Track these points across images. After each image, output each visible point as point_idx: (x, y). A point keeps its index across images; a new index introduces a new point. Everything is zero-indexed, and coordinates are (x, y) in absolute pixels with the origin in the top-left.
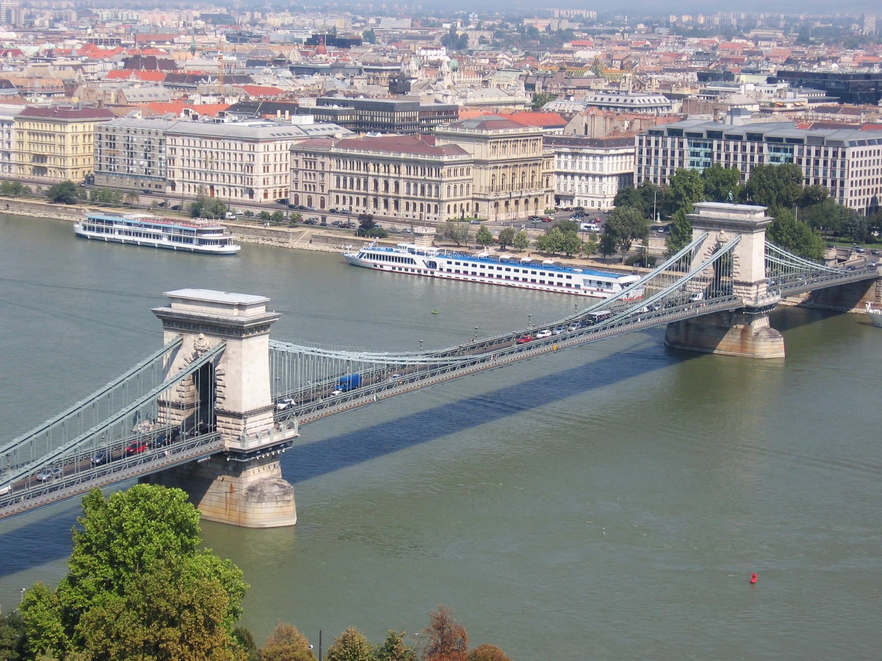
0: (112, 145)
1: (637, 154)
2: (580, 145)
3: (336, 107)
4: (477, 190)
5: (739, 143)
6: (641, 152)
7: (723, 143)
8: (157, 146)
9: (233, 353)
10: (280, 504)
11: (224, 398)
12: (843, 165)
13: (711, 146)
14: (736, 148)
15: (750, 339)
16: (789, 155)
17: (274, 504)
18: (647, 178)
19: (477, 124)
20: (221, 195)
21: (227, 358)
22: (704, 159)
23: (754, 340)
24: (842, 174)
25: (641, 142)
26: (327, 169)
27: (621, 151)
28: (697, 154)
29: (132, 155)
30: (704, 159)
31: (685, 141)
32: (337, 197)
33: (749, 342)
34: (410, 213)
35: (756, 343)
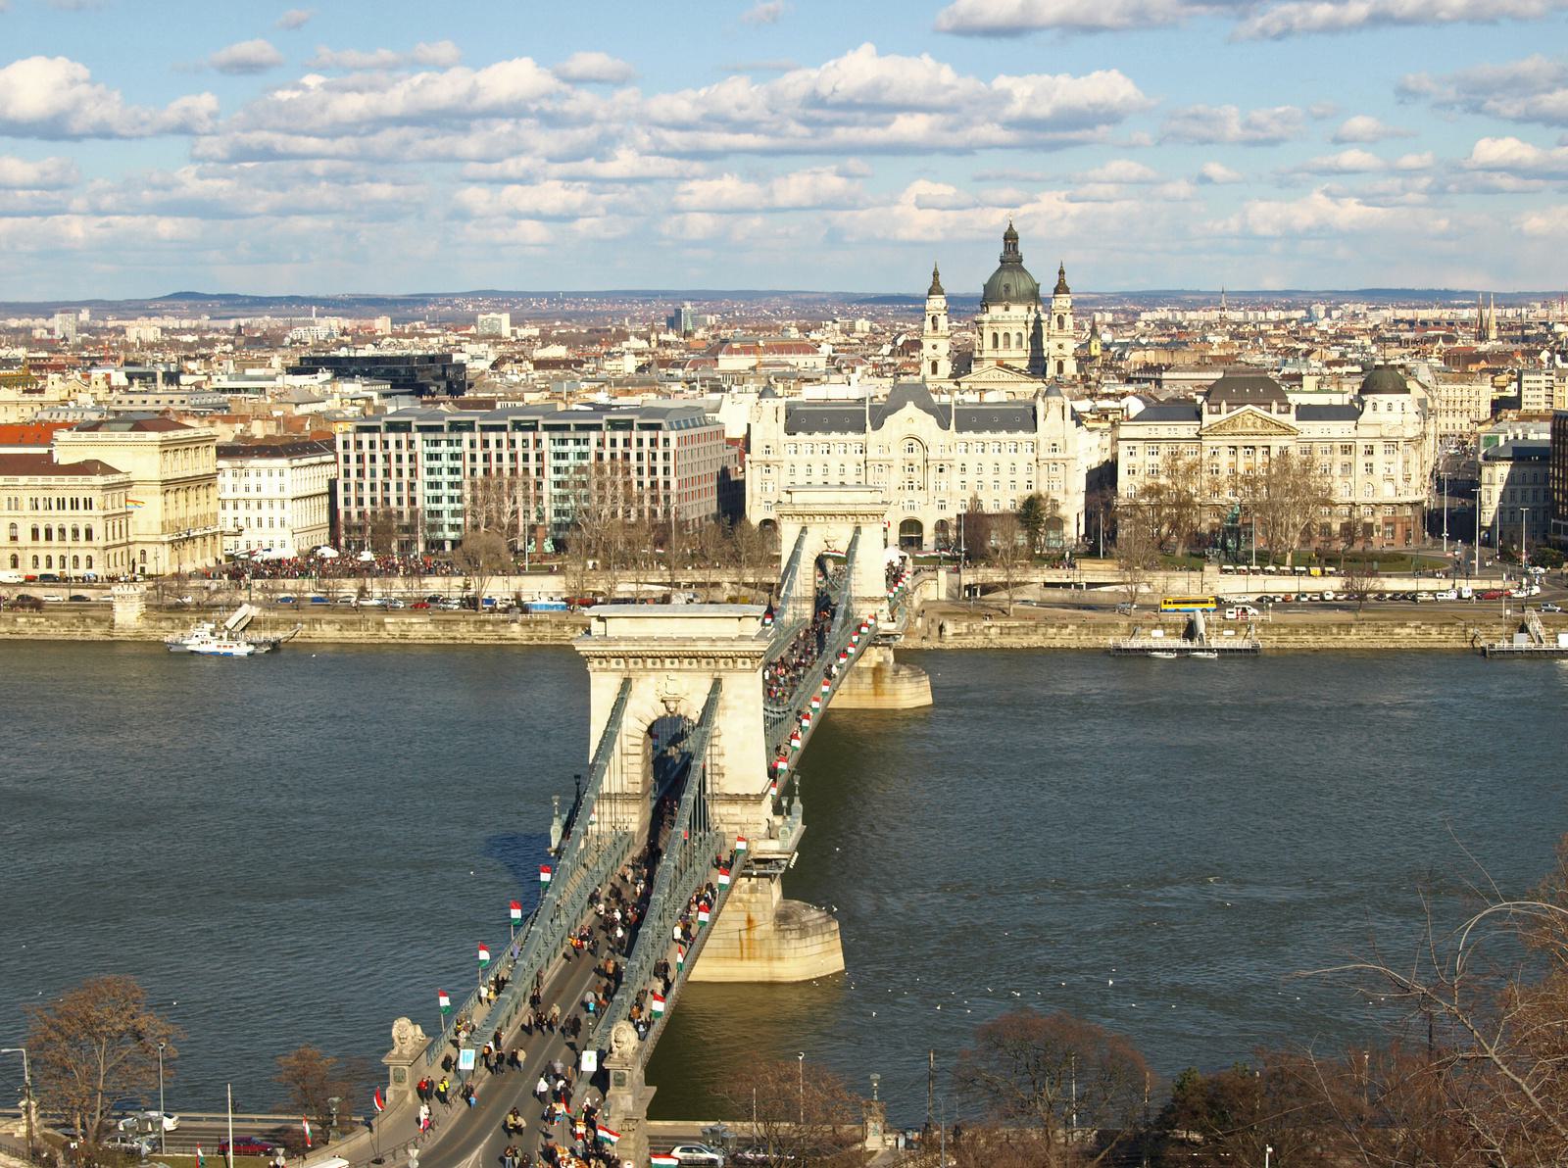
2: (243, 456)
4: (142, 528)
5: (504, 436)
6: (347, 459)
12: (666, 456)
13: (459, 442)
14: (499, 443)
15: (887, 680)
19: (131, 425)
21: (725, 708)
23: (894, 682)
24: (666, 470)
25: (346, 445)
27: (305, 461)
28: (438, 457)
30: (452, 464)
33: (887, 685)
35: (898, 686)
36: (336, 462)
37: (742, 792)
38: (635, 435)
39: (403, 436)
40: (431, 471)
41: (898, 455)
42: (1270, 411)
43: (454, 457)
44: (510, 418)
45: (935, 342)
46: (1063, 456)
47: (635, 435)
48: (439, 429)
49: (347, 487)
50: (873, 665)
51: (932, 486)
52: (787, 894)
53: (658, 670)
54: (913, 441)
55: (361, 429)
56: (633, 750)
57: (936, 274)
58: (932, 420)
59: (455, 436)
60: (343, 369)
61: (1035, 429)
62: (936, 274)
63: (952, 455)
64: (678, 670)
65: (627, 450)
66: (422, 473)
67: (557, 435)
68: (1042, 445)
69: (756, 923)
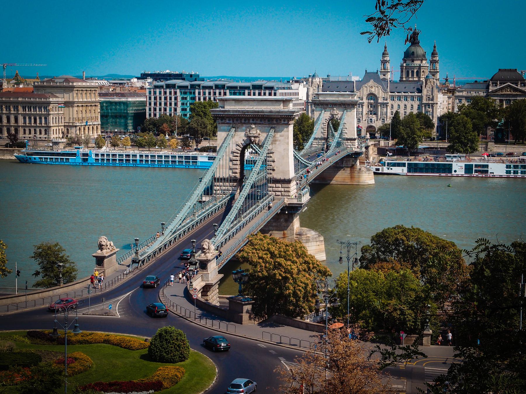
1: (148, 100)
4: (67, 121)
5: (212, 91)
6: (150, 98)
7: (201, 91)
9: (281, 136)
10: (318, 243)
11: (274, 170)
13: (194, 93)
14: (210, 93)
15: (356, 172)
17: (315, 243)
19: (63, 80)
21: (276, 141)
30: (191, 101)
31: (178, 91)
33: (356, 174)
34: (27, 135)
35: (361, 175)
37: (282, 178)
39: (173, 90)
40: (183, 104)
41: (365, 101)
42: (517, 86)
45: (384, 73)
46: (432, 102)
47: (263, 92)
49: (150, 109)
51: (379, 113)
52: (302, 225)
53: (247, 123)
54: (372, 96)
56: (234, 158)
57: (385, 48)
58: (380, 87)
61: (420, 91)
62: (385, 48)
63: (388, 101)
64: (255, 124)
66: (179, 104)
68: (424, 98)
69: (287, 235)
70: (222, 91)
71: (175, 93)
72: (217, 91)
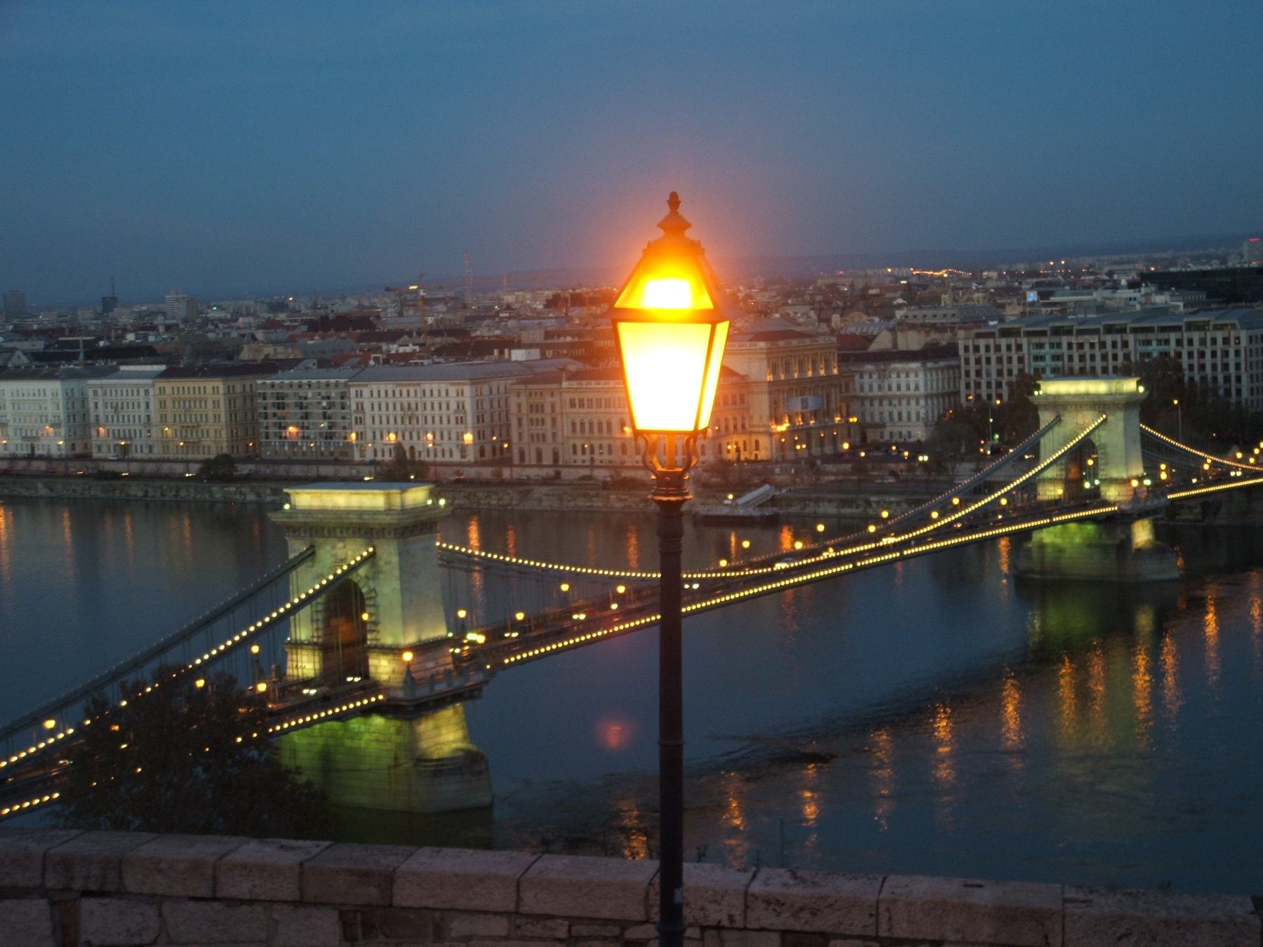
0: (281, 406)
3: (569, 339)
5: (1095, 339)
6: (967, 361)
8: (338, 401)
12: (1237, 353)
13: (1059, 345)
16: (1163, 348)
18: (978, 397)
20: (424, 457)
22: (1053, 364)
24: (1238, 366)
25: (966, 349)
26: (558, 410)
27: (942, 364)
28: (1042, 358)
29: (306, 416)
30: (1053, 364)
32: (574, 447)
36: (959, 367)
38: (1209, 335)
39: (1012, 341)
43: (1056, 358)
44: (1051, 325)
47: (1209, 335)
48: (1043, 333)
49: (968, 385)
50: (1117, 542)
55: (979, 336)
59: (1055, 339)
60: (1163, 281)
65: (1179, 349)
67: (1142, 336)
70: (1118, 338)
71: (1019, 347)
72: (1109, 339)
